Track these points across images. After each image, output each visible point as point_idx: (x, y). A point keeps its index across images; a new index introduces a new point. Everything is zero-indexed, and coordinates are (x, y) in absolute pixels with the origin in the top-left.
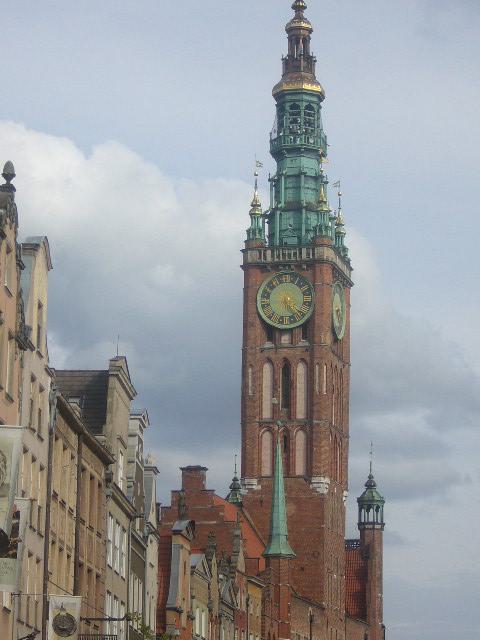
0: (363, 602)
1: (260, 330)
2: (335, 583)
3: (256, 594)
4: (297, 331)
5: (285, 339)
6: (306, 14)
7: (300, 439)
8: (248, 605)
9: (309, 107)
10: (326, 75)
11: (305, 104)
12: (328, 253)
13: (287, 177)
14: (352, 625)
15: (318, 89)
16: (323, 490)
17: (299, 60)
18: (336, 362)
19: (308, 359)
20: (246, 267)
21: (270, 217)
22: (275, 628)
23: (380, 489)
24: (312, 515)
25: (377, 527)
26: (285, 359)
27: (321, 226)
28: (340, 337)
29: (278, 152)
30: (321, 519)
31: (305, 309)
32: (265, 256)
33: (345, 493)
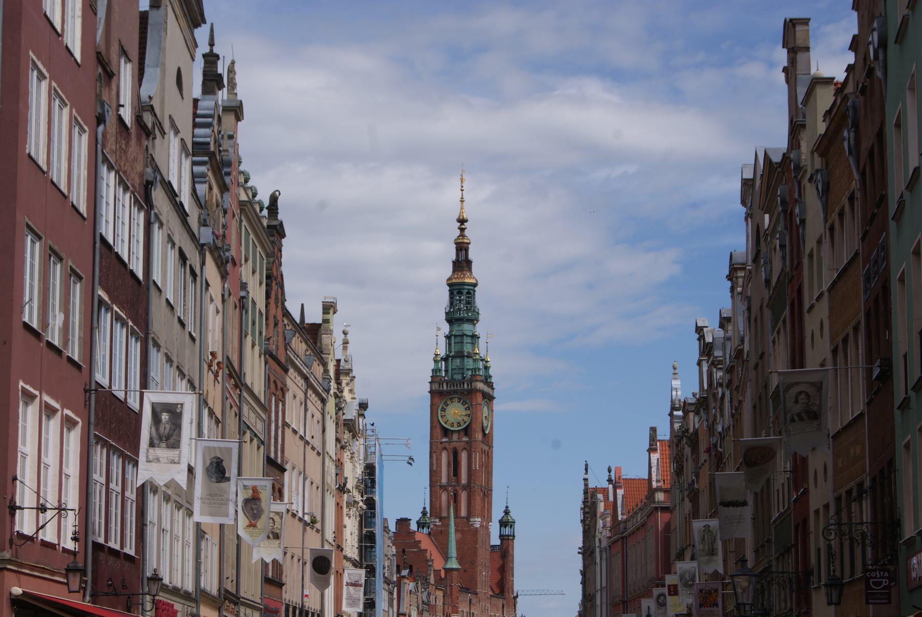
0: (502, 588)
1: (440, 432)
2: (485, 576)
3: (440, 594)
6: (466, 233)
7: (463, 496)
9: (468, 293)
10: (479, 272)
12: (480, 386)
13: (456, 336)
15: (474, 281)
17: (462, 263)
18: (486, 448)
21: (445, 359)
23: (513, 515)
24: (470, 540)
26: (455, 448)
27: (475, 369)
31: (466, 419)
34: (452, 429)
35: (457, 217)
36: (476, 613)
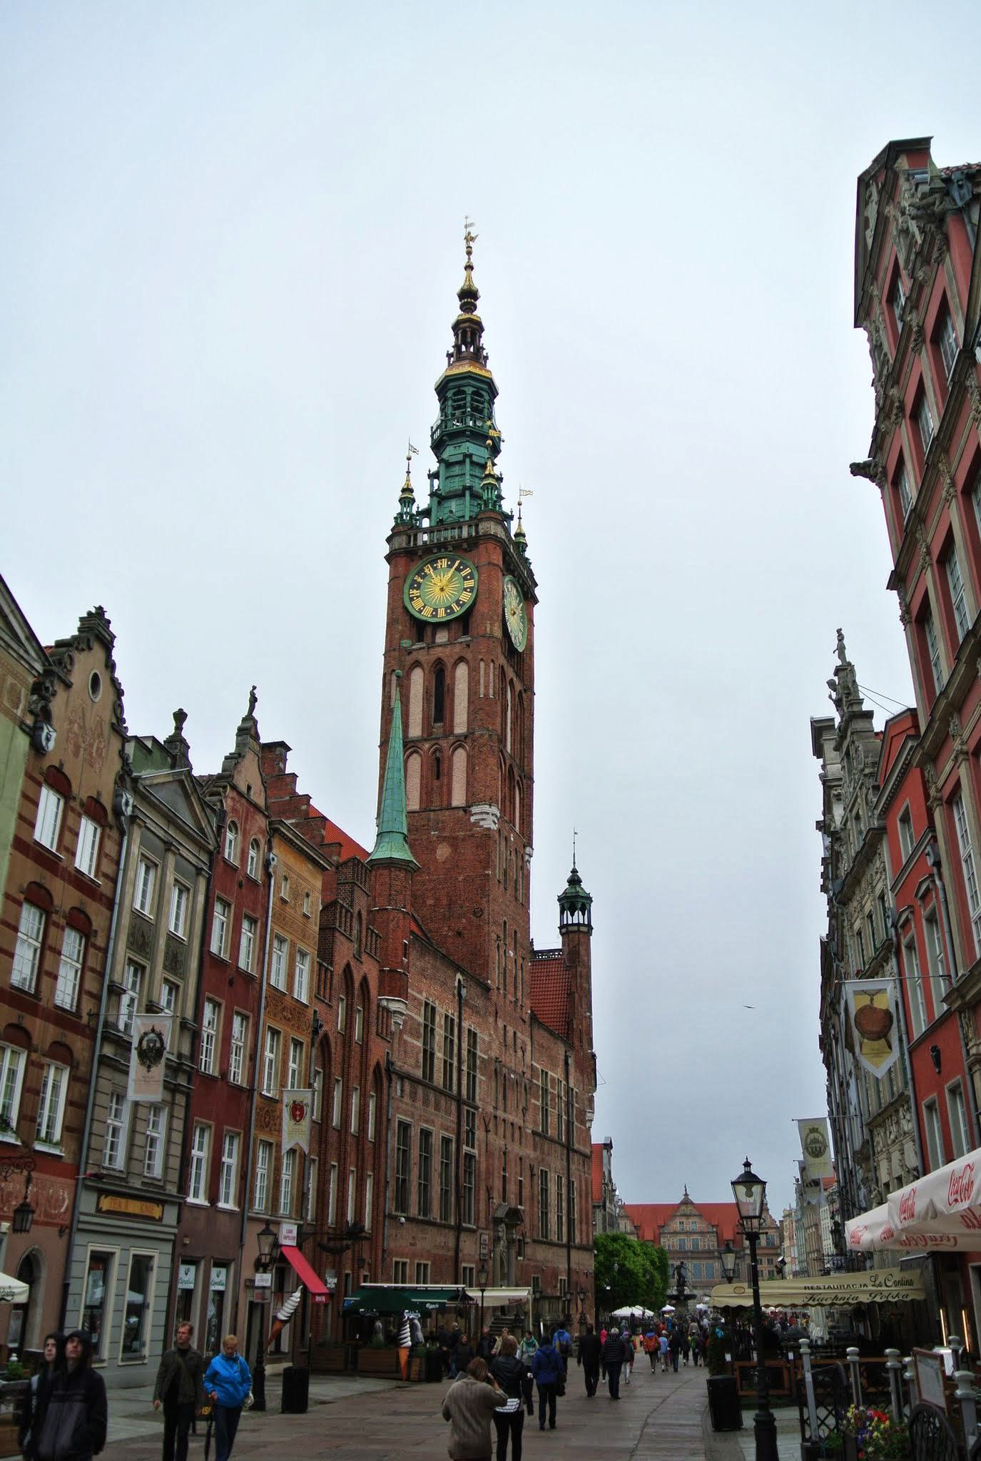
1: (408, 630)
4: (453, 626)
5: (442, 637)
7: (460, 758)
8: (269, 876)
11: (472, 389)
14: (541, 1035)
16: (490, 823)
18: (510, 674)
19: (469, 656)
20: (389, 558)
21: (426, 513)
22: (368, 969)
23: (587, 886)
25: (583, 929)
29: (438, 447)
30: (487, 864)
32: (415, 539)
33: (528, 850)
35: (459, 284)
36: (482, 1036)
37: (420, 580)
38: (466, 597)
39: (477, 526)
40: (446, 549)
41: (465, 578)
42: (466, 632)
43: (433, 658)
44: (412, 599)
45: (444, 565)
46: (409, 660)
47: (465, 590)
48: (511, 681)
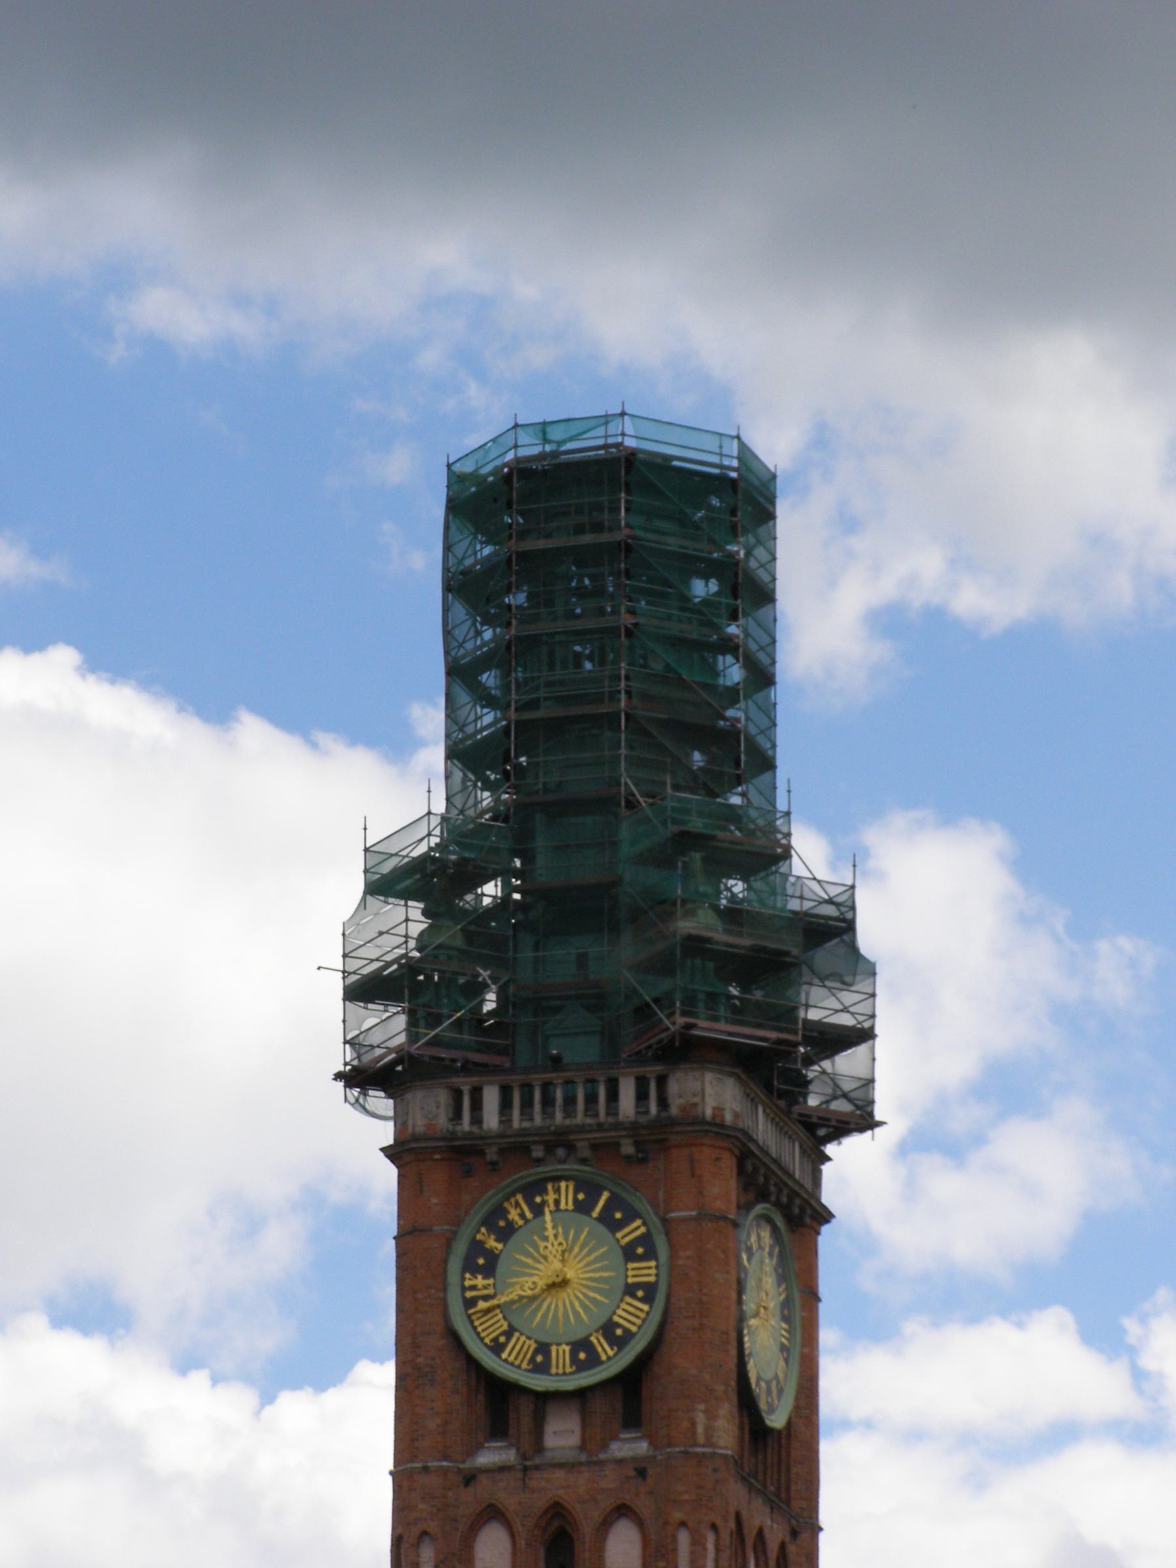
5: (562, 1434)
18: (759, 1516)
19: (645, 1506)
26: (557, 1510)
28: (777, 1420)
32: (477, 1105)
34: (539, 1383)
37: (492, 1243)
38: (634, 1316)
39: (662, 1081)
40: (570, 1147)
41: (629, 1253)
42: (633, 1419)
43: (540, 1503)
44: (470, 1303)
45: (567, 1203)
46: (469, 1500)
47: (630, 1290)
48: (760, 1534)
